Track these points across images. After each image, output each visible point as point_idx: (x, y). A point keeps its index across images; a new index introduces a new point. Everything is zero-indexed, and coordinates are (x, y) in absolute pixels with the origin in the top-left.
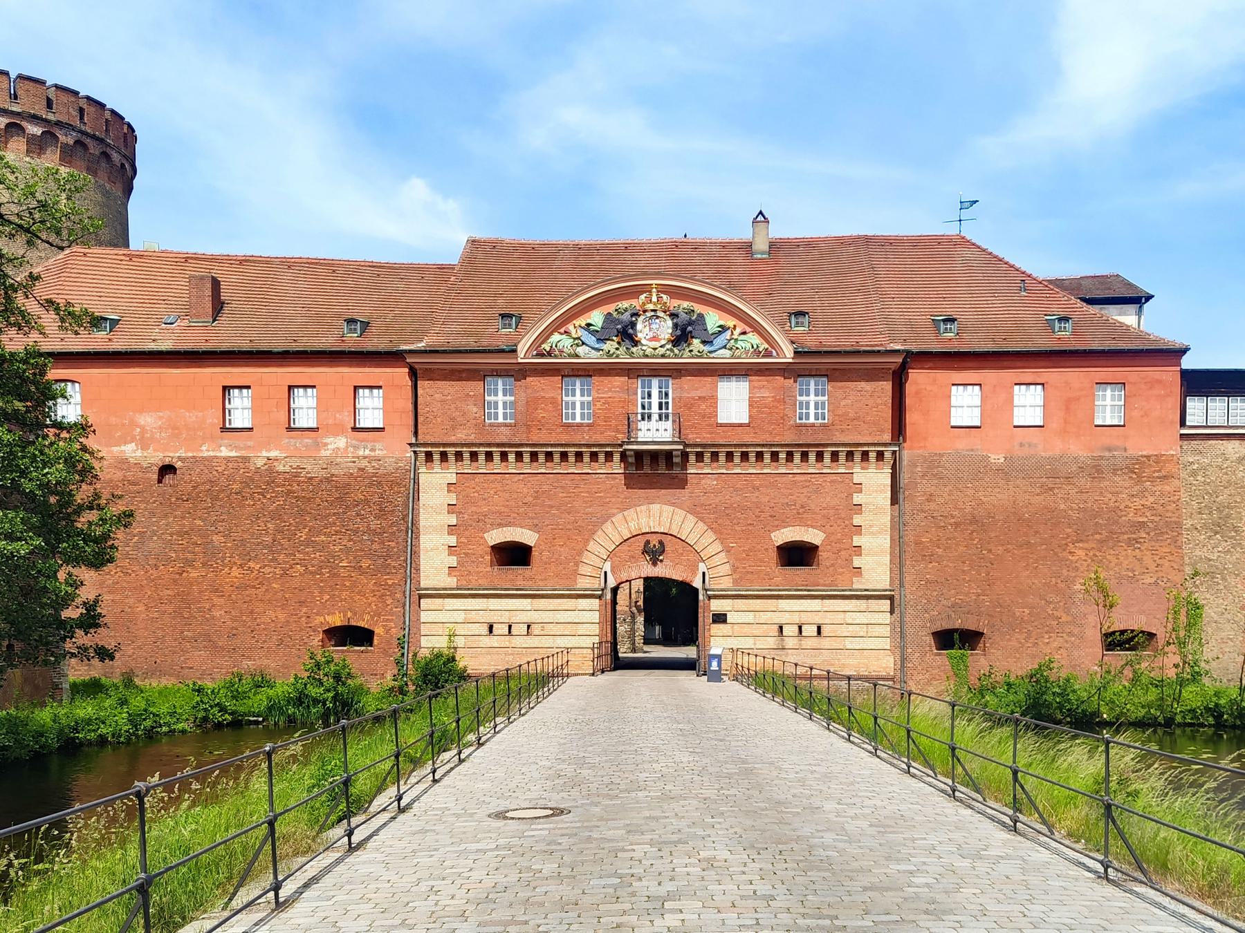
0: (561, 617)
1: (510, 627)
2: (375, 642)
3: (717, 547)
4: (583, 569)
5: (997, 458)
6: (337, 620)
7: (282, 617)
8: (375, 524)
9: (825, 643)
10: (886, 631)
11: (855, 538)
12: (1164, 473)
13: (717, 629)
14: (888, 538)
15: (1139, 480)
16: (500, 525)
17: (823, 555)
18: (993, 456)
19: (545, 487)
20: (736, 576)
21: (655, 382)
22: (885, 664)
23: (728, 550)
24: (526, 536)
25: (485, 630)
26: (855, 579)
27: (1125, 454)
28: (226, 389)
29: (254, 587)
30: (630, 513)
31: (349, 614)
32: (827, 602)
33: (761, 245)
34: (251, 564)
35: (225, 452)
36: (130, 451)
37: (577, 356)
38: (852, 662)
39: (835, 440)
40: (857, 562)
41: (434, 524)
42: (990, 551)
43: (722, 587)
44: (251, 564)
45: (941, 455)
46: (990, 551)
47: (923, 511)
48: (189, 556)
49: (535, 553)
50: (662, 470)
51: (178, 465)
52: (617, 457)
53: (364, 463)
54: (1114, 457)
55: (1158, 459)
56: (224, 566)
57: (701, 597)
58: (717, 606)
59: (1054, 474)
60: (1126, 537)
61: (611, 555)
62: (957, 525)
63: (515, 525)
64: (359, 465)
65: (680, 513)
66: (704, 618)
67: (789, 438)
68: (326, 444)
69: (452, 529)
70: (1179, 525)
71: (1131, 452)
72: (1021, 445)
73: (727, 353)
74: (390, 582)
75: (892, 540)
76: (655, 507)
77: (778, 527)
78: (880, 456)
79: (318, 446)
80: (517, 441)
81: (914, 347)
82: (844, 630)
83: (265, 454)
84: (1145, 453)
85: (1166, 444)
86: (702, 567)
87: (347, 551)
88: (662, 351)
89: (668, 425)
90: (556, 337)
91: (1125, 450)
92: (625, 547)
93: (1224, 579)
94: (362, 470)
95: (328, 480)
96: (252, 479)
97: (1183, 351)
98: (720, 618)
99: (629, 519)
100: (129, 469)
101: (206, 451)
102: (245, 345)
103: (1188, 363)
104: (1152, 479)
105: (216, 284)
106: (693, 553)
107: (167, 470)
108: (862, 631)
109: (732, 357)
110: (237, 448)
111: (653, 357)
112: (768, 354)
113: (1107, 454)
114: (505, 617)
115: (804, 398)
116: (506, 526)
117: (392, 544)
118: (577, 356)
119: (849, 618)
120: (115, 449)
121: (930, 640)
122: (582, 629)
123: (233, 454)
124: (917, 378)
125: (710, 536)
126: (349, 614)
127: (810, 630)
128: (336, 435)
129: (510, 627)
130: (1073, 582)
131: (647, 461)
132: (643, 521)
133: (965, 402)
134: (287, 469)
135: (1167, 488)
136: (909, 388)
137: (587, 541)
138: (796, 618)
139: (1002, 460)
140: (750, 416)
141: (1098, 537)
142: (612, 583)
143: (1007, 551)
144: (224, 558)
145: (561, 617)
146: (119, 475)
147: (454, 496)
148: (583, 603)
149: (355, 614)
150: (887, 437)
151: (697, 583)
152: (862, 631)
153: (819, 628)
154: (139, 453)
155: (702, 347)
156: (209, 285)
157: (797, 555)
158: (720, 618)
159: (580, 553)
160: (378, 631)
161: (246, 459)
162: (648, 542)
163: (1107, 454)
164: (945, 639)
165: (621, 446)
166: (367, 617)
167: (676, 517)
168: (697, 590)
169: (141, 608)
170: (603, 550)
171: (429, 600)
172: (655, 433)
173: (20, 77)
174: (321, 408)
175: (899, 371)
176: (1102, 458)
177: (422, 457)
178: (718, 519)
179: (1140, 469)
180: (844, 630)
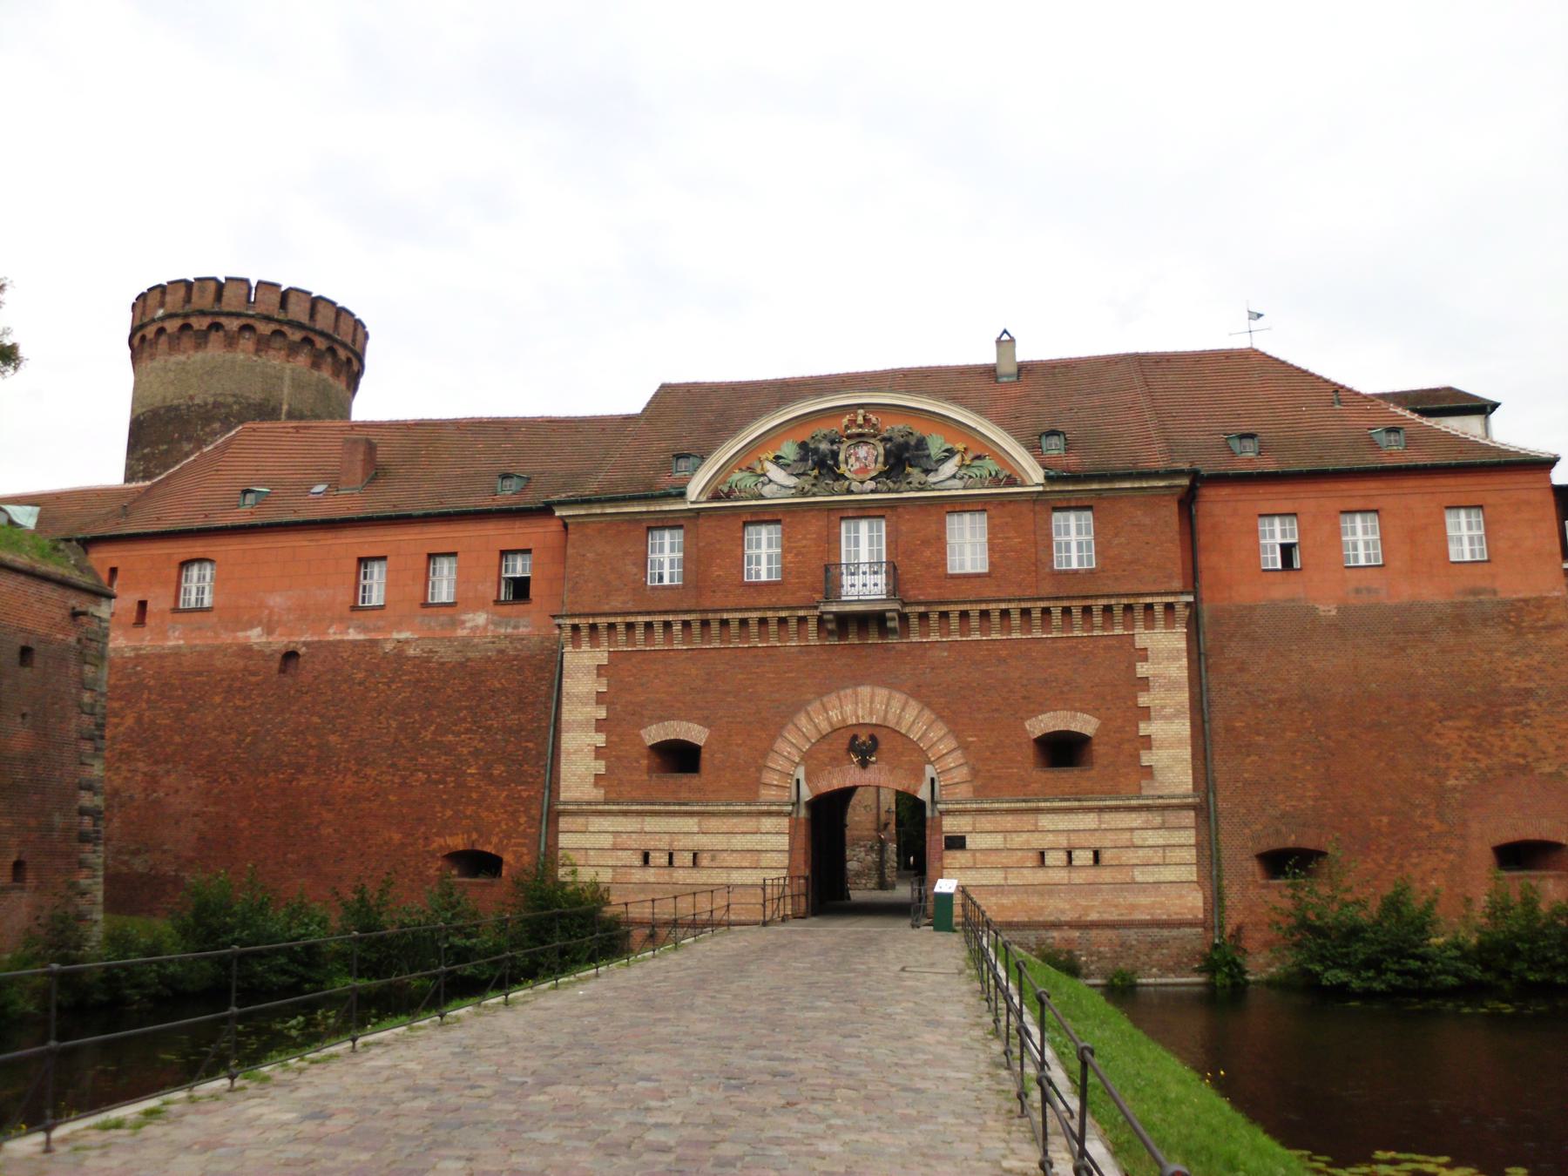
0: (739, 842)
1: (671, 855)
2: (504, 873)
3: (951, 743)
4: (771, 778)
6: (458, 842)
7: (397, 837)
8: (513, 719)
9: (1106, 875)
10: (1190, 855)
11: (1142, 725)
12: (1549, 621)
13: (955, 858)
14: (1188, 723)
15: (1519, 631)
16: (661, 719)
17: (1099, 749)
18: (1321, 608)
19: (721, 667)
20: (978, 783)
21: (864, 525)
22: (1193, 902)
23: (964, 747)
24: (696, 734)
25: (638, 861)
26: (1144, 783)
27: (1498, 598)
28: (363, 561)
29: (368, 799)
30: (831, 700)
31: (475, 836)
32: (1107, 817)
34: (368, 771)
35: (353, 635)
36: (255, 636)
37: (762, 497)
38: (1144, 900)
39: (1106, 591)
40: (1146, 759)
41: (580, 717)
42: (1328, 737)
43: (959, 797)
44: (368, 771)
45: (1252, 608)
46: (1328, 737)
47: (1234, 685)
48: (302, 760)
49: (705, 755)
50: (873, 639)
51: (303, 650)
52: (812, 625)
53: (504, 644)
54: (1481, 602)
55: (1540, 603)
56: (337, 772)
57: (929, 813)
58: (951, 825)
59: (1405, 626)
60: (1508, 710)
61: (807, 757)
62: (1281, 703)
63: (680, 718)
64: (498, 646)
65: (898, 699)
66: (934, 843)
67: (1047, 588)
68: (463, 622)
69: (600, 725)
72: (1358, 591)
73: (956, 482)
74: (525, 794)
75: (1193, 726)
76: (865, 691)
77: (1034, 713)
79: (455, 623)
80: (685, 607)
81: (1205, 469)
82: (1130, 857)
83: (396, 636)
84: (1521, 595)
86: (930, 771)
87: (476, 753)
88: (871, 485)
89: (881, 579)
90: (737, 476)
91: (1495, 593)
92: (825, 747)
94: (501, 651)
95: (462, 665)
96: (377, 666)
97: (1550, 463)
98: (956, 843)
99: (829, 706)
100: (250, 658)
101: (333, 634)
102: (389, 511)
103: (1559, 476)
104: (1533, 629)
105: (371, 448)
106: (916, 756)
107: (290, 656)
108: (1157, 857)
110: (365, 630)
111: (862, 493)
112: (1011, 481)
113: (1471, 599)
114: (664, 843)
116: (668, 719)
117: (531, 745)
118: (762, 497)
119: (1138, 838)
120: (241, 634)
121: (1254, 867)
122: (766, 860)
123: (361, 637)
124: (1217, 505)
125: (939, 731)
126: (475, 836)
127: (1083, 857)
128: (475, 611)
129: (671, 855)
130: (1445, 776)
131: (853, 628)
132: (849, 708)
134: (418, 652)
135: (1557, 641)
136: (1203, 523)
137: (773, 739)
138: (1063, 841)
139: (1334, 613)
140: (991, 564)
141: (1471, 711)
142: (806, 794)
143: (1352, 736)
144: (338, 764)
145: (739, 842)
146: (241, 664)
147: (604, 681)
148: (768, 823)
149: (480, 836)
150: (1177, 585)
151: (923, 794)
152: (1157, 857)
153: (1096, 854)
154: (264, 639)
155: (923, 477)
156: (362, 449)
157: (1063, 751)
158: (956, 843)
159: (764, 755)
160: (507, 857)
161: (373, 643)
162: (855, 737)
163: (1471, 599)
164: (1277, 862)
165: (816, 608)
166: (495, 840)
167: (877, 699)
168: (922, 804)
169: (244, 823)
170: (794, 751)
171: (569, 819)
172: (864, 585)
173: (259, 283)
174: (462, 581)
175: (1192, 491)
176: (1464, 604)
177: (568, 632)
178: (951, 707)
180: (1130, 857)
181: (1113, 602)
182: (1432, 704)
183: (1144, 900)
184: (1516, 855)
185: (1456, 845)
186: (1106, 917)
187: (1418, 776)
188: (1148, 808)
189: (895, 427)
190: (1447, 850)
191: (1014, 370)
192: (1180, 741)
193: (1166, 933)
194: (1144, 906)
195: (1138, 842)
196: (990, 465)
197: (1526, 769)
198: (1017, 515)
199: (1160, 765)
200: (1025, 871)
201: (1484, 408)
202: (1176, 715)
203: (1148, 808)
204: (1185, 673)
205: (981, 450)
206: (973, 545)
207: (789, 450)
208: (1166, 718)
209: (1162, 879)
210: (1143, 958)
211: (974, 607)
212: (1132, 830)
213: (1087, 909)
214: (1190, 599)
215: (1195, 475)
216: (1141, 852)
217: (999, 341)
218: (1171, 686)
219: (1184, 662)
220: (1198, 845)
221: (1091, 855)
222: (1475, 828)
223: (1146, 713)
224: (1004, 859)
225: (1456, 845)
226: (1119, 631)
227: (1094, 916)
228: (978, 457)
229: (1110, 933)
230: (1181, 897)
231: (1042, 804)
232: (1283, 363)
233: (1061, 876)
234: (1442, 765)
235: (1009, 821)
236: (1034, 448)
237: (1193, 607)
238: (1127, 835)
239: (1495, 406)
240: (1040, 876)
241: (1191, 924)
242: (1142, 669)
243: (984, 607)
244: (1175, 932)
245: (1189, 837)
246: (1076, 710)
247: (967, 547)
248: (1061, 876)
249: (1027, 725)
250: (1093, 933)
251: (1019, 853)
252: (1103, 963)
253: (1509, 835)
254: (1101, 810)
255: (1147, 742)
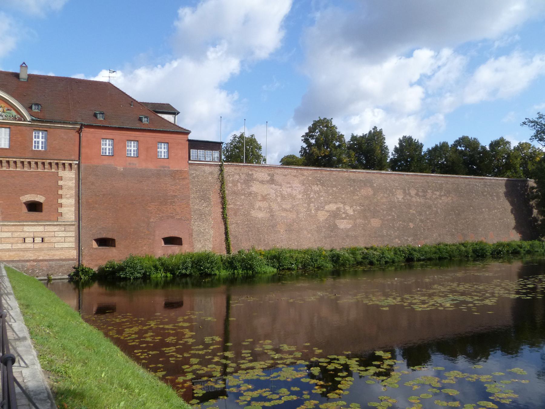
5: (120, 169)
9: (45, 245)
10: (73, 239)
17: (44, 207)
22: (74, 254)
32: (46, 227)
55: (181, 172)
62: (104, 195)
70: (189, 197)
71: (171, 169)
72: (130, 164)
77: (23, 195)
78: (70, 165)
82: (54, 240)
85: (183, 166)
91: (169, 168)
93: (205, 217)
103: (191, 137)
109: (3, 120)
113: (162, 169)
115: (37, 140)
127: (38, 240)
133: (107, 146)
136: (83, 139)
140: (10, 145)
153: (42, 239)
163: (162, 169)
176: (160, 170)
179: (175, 175)
180: (54, 240)
181: (52, 161)
182: (148, 198)
183: (58, 253)
184: (171, 241)
185: (152, 238)
186: (45, 258)
187: (143, 218)
188: (60, 225)
190: (149, 239)
191: (26, 77)
192: (71, 205)
193: (64, 263)
194: (58, 255)
195: (56, 235)
197: (172, 217)
199: (64, 212)
200: (18, 244)
201: (175, 113)
202: (70, 197)
203: (60, 225)
204: (74, 185)
206: (5, 139)
208: (67, 198)
209: (63, 246)
210: (56, 270)
211: (4, 159)
212: (55, 232)
213: (38, 256)
214: (77, 162)
215: (82, 125)
216: (57, 239)
217: (21, 66)
218: (69, 188)
219: (74, 181)
220: (75, 236)
221: (41, 239)
222: (157, 232)
223: (61, 196)
224: (11, 241)
225: (152, 238)
226: (53, 170)
227: (41, 258)
228: (8, 110)
229: (46, 263)
230: (69, 252)
231: (25, 223)
232: (118, 89)
233: (31, 246)
234: (150, 215)
235: (13, 228)
236: (29, 108)
237: (79, 165)
238: (53, 233)
239: (178, 113)
240: (23, 246)
241: (72, 260)
242: (60, 183)
243: (8, 159)
244: (67, 263)
245: (73, 234)
246: (38, 194)
248: (31, 246)
249: (21, 198)
250: (41, 263)
251: (17, 239)
252: (44, 272)
253: (167, 235)
254: (44, 225)
255: (61, 205)
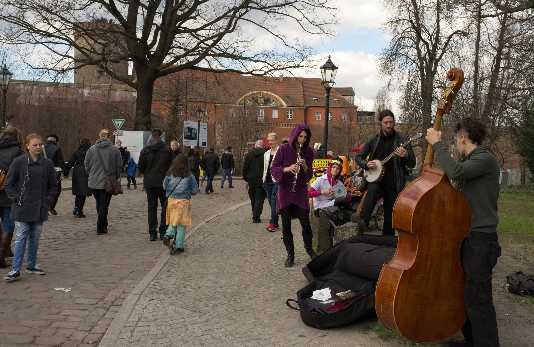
33: (281, 79)
136: (308, 113)
189: (266, 96)
196: (279, 103)
198: (282, 111)
205: (278, 101)
207: (251, 98)
247: (275, 114)
